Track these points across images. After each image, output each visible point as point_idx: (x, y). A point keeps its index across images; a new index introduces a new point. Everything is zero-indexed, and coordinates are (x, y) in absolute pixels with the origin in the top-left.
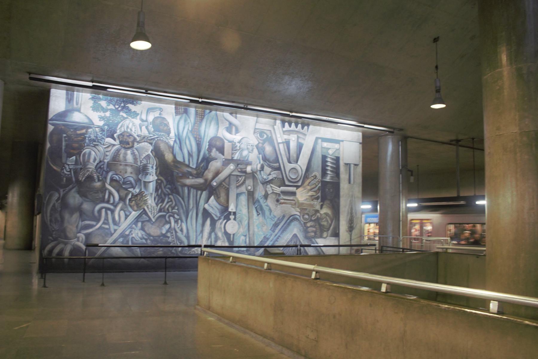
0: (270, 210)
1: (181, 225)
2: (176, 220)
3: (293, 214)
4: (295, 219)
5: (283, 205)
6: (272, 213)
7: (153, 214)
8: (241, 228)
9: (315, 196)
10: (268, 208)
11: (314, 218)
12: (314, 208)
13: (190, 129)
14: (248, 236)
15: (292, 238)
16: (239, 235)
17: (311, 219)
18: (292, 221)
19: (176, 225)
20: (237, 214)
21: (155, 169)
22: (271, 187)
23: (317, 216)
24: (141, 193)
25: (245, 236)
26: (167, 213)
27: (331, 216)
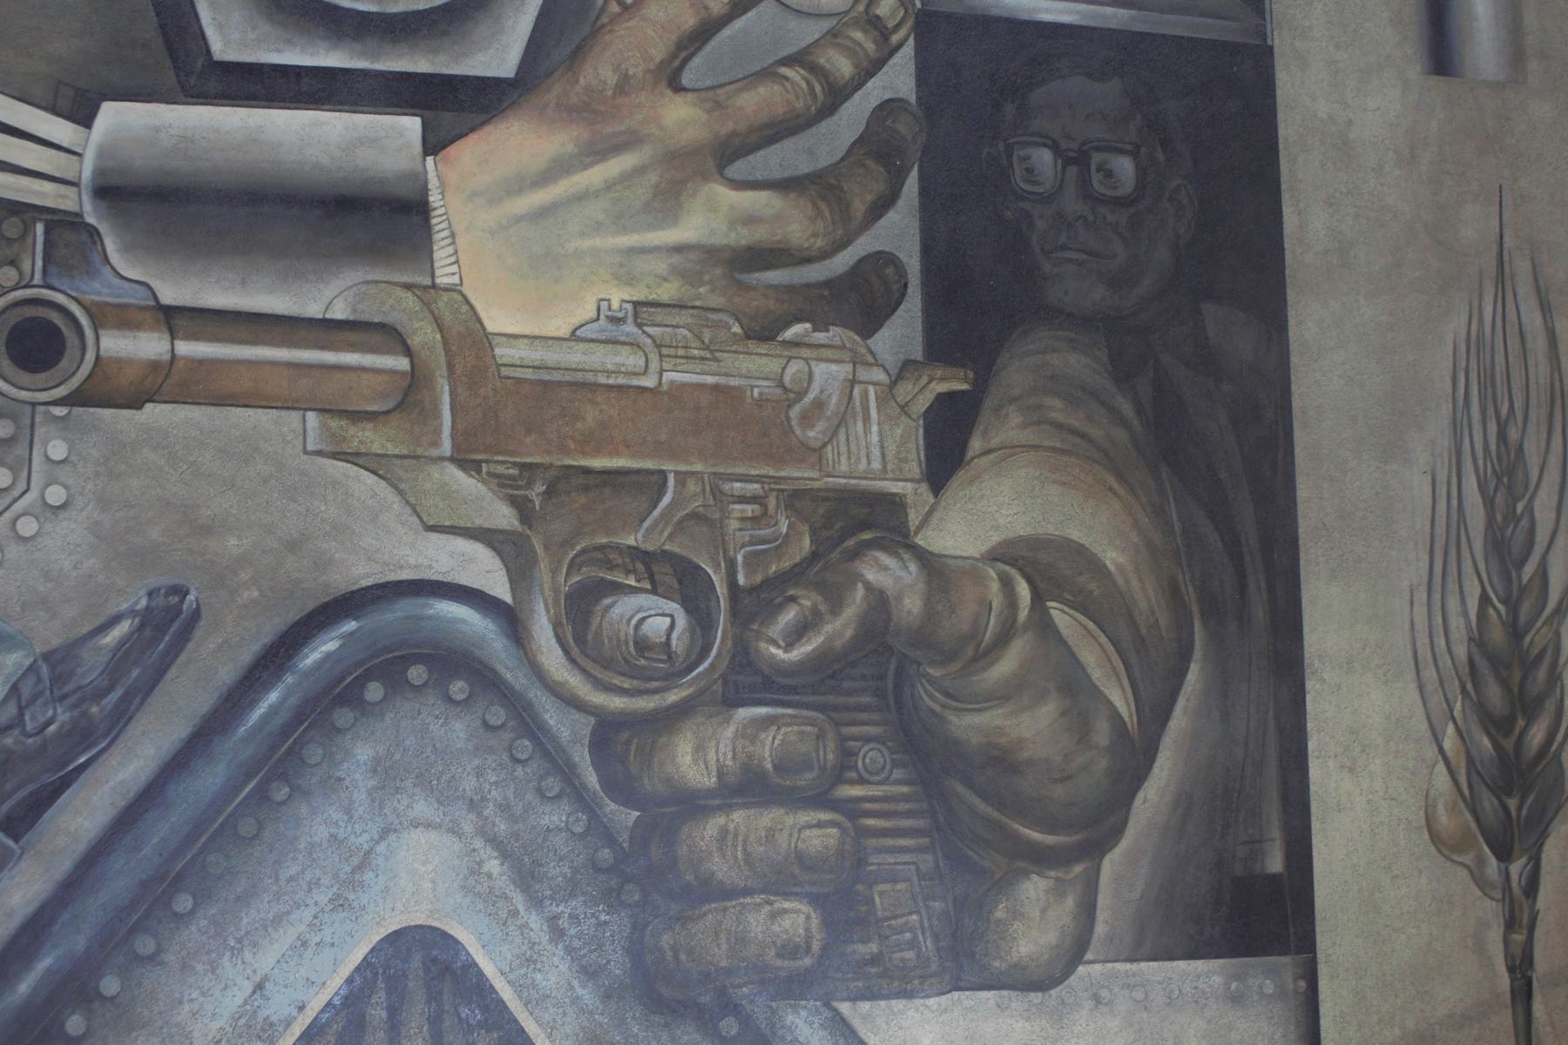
3: (363, 574)
4: (417, 674)
5: (153, 412)
9: (805, 259)
11: (800, 631)
12: (801, 474)
15: (353, 999)
17: (743, 656)
23: (856, 600)
27: (1145, 595)
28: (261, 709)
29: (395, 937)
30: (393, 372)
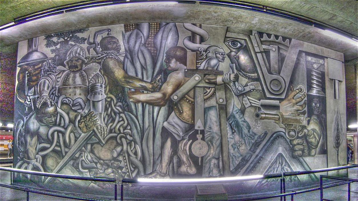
0: (249, 127)
1: (135, 147)
2: (128, 141)
3: (277, 131)
5: (265, 120)
6: (251, 131)
7: (103, 135)
8: (212, 150)
10: (245, 124)
13: (143, 42)
14: (221, 159)
16: (209, 158)
18: (275, 139)
19: (129, 147)
20: (206, 132)
21: (104, 88)
22: (249, 99)
24: (90, 113)
25: (218, 159)
26: (118, 134)
28: (271, 139)
29: (279, 154)
30: (278, 117)
